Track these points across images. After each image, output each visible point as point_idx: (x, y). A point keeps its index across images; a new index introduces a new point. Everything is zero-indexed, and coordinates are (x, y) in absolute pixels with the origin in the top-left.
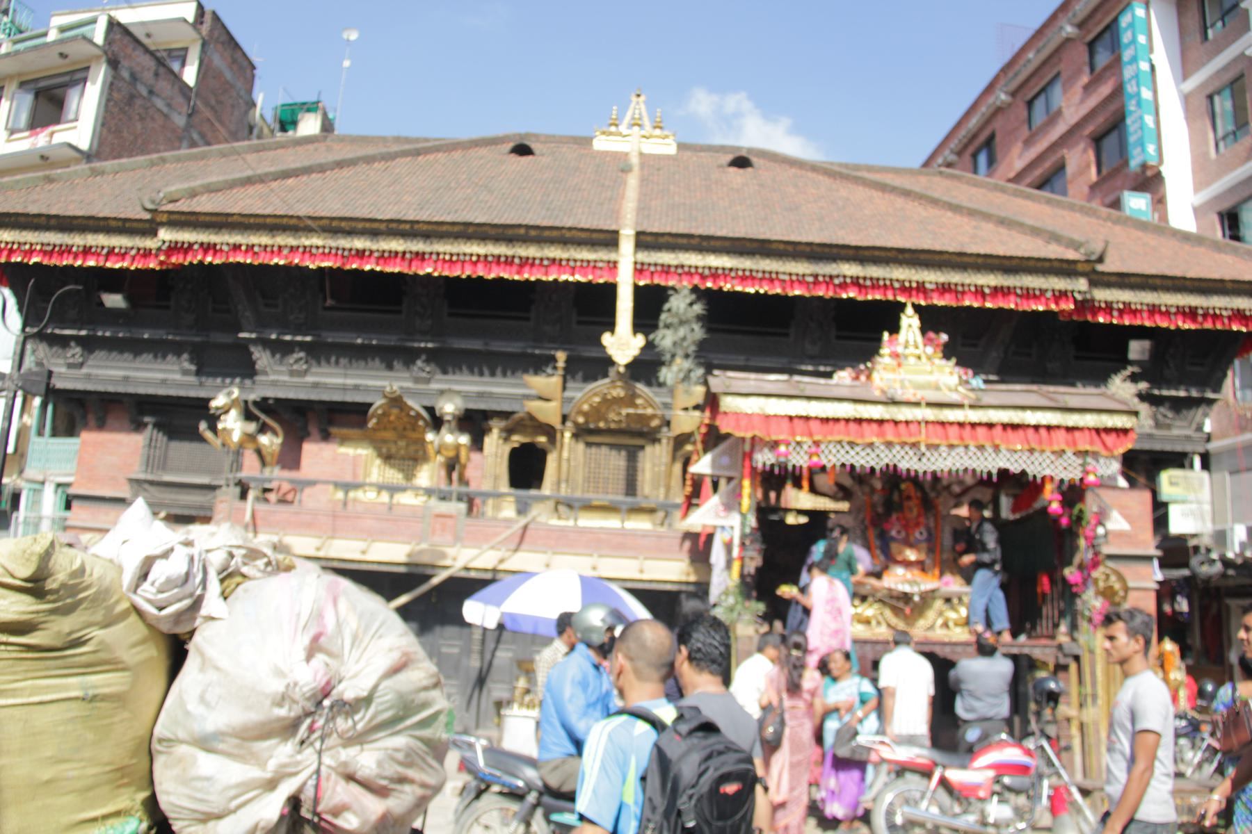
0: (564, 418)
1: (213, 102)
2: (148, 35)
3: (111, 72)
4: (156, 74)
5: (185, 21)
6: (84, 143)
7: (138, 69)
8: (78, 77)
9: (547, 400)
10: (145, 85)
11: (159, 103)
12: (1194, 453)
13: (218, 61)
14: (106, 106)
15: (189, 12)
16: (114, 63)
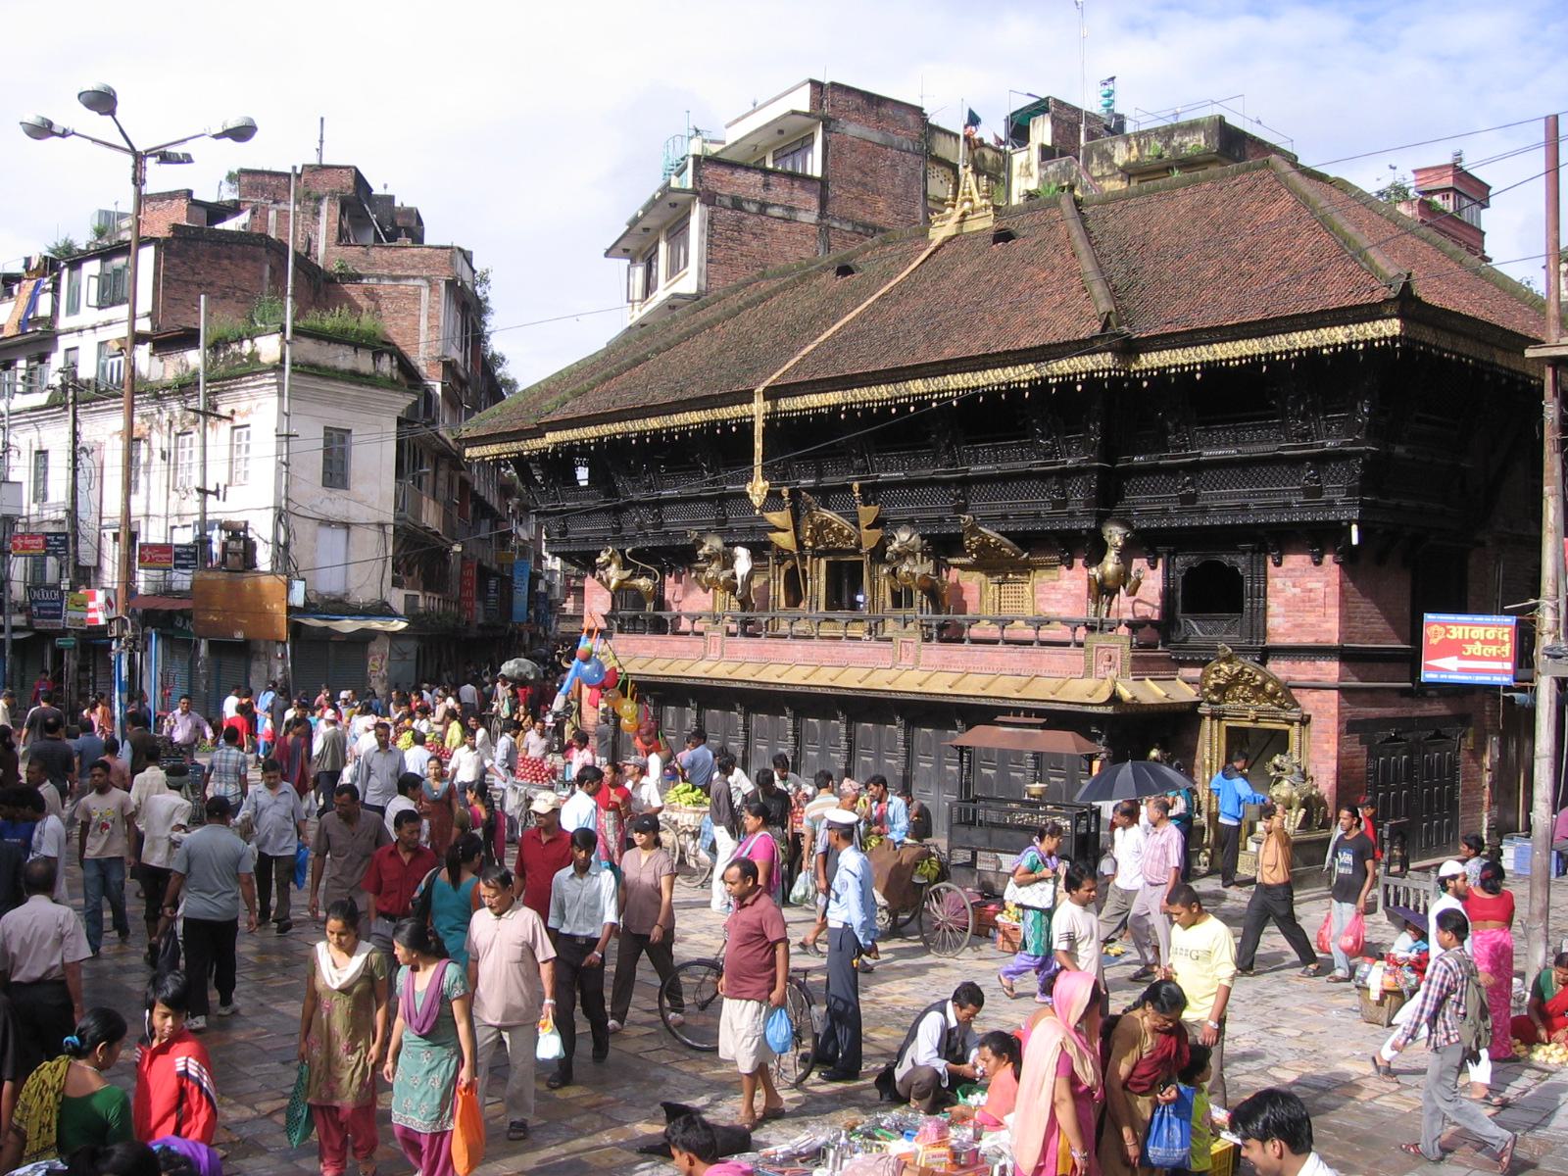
0: (800, 545)
1: (857, 176)
2: (781, 132)
3: (705, 208)
4: (766, 186)
5: (794, 113)
6: (693, 290)
7: (738, 192)
8: (677, 230)
9: (785, 531)
10: (754, 202)
11: (776, 212)
12: (1350, 522)
13: (853, 130)
14: (710, 243)
15: (802, 101)
16: (709, 199)
